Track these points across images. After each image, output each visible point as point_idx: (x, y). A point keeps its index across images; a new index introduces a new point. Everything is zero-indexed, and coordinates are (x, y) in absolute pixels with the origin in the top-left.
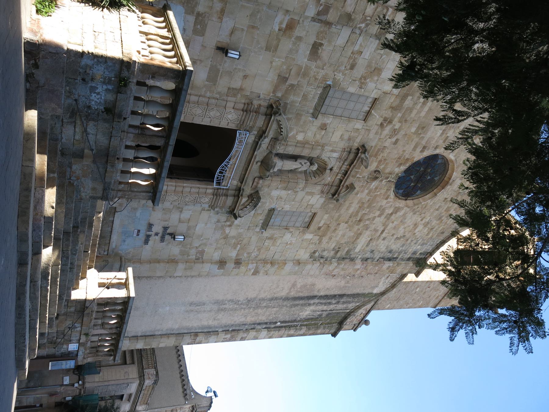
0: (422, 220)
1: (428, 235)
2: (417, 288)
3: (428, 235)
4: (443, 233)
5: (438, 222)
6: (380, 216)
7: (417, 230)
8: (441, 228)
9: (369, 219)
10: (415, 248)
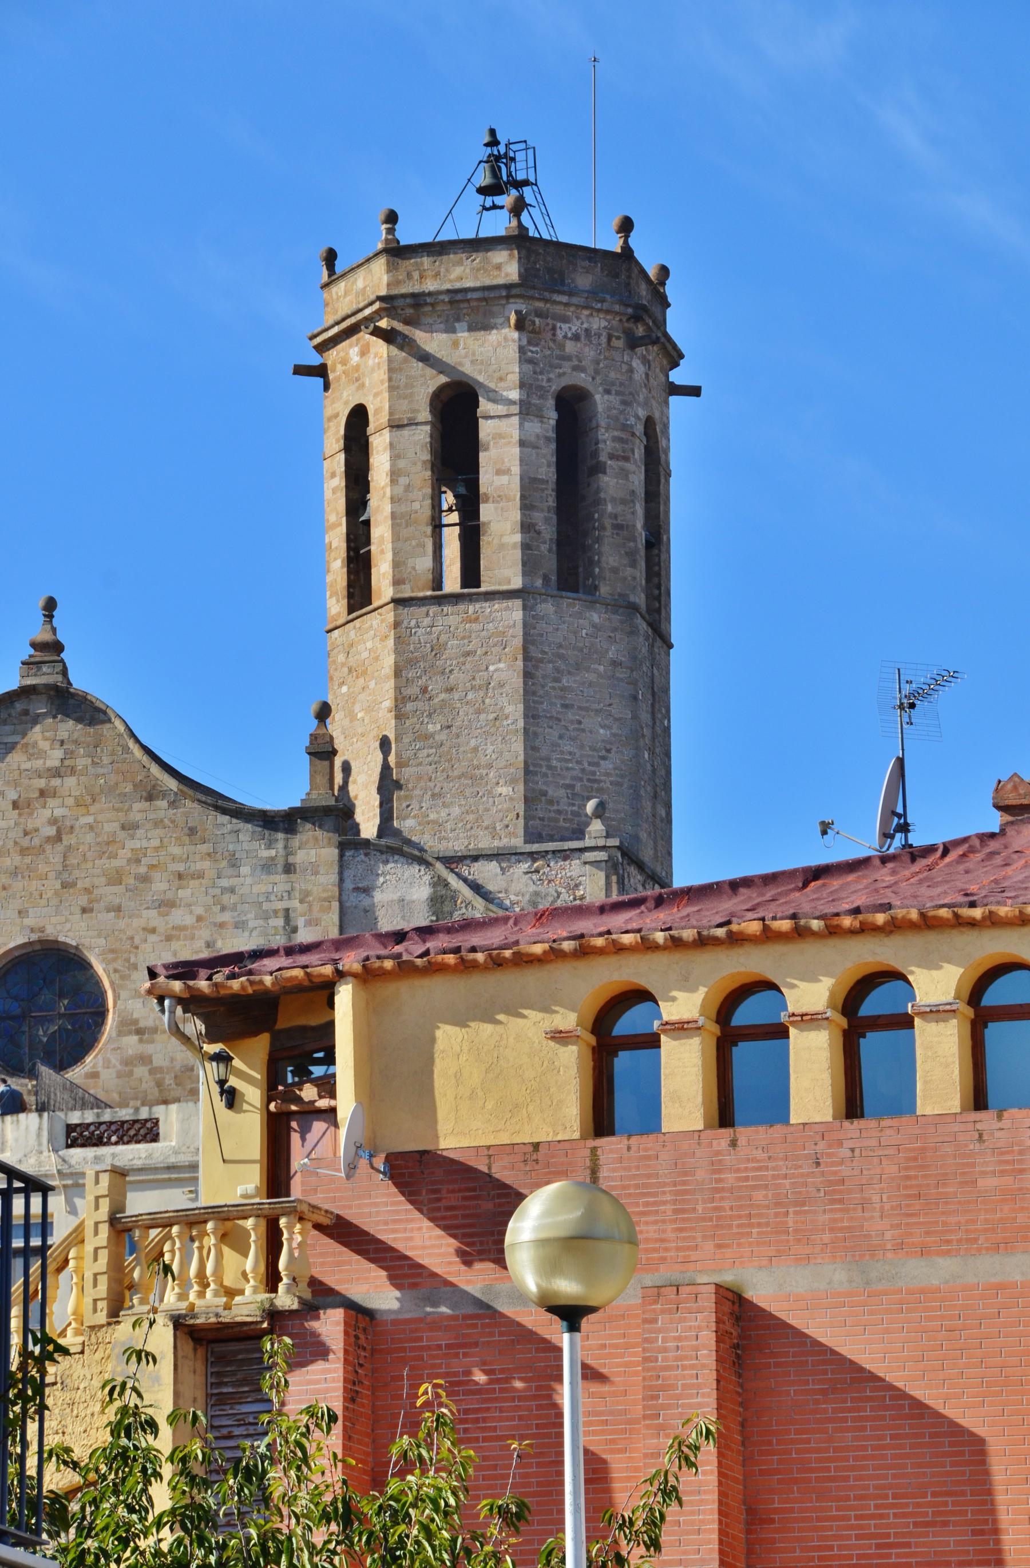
0: (153, 931)
1: (200, 875)
2: (428, 736)
3: (200, 875)
4: (192, 831)
5: (156, 875)
6: (145, 1059)
7: (189, 920)
8: (176, 850)
9: (159, 1084)
10: (249, 880)
